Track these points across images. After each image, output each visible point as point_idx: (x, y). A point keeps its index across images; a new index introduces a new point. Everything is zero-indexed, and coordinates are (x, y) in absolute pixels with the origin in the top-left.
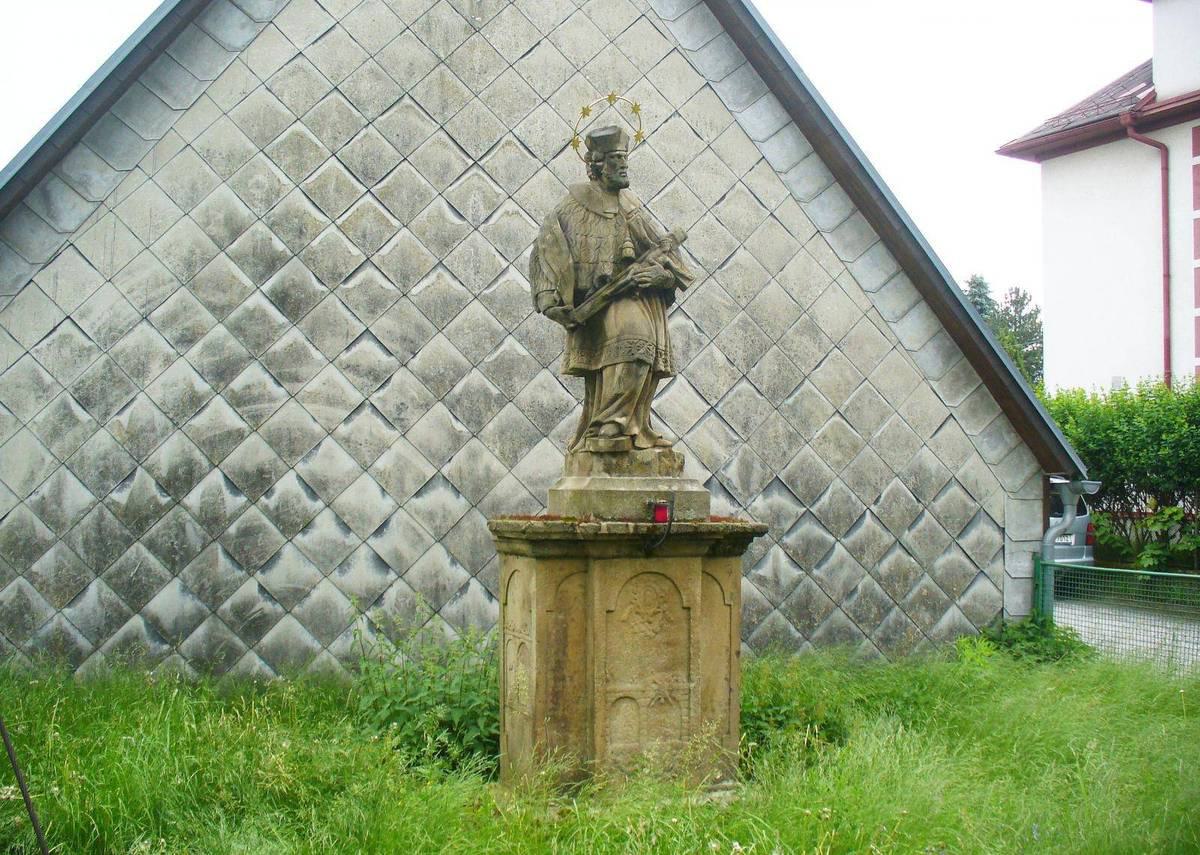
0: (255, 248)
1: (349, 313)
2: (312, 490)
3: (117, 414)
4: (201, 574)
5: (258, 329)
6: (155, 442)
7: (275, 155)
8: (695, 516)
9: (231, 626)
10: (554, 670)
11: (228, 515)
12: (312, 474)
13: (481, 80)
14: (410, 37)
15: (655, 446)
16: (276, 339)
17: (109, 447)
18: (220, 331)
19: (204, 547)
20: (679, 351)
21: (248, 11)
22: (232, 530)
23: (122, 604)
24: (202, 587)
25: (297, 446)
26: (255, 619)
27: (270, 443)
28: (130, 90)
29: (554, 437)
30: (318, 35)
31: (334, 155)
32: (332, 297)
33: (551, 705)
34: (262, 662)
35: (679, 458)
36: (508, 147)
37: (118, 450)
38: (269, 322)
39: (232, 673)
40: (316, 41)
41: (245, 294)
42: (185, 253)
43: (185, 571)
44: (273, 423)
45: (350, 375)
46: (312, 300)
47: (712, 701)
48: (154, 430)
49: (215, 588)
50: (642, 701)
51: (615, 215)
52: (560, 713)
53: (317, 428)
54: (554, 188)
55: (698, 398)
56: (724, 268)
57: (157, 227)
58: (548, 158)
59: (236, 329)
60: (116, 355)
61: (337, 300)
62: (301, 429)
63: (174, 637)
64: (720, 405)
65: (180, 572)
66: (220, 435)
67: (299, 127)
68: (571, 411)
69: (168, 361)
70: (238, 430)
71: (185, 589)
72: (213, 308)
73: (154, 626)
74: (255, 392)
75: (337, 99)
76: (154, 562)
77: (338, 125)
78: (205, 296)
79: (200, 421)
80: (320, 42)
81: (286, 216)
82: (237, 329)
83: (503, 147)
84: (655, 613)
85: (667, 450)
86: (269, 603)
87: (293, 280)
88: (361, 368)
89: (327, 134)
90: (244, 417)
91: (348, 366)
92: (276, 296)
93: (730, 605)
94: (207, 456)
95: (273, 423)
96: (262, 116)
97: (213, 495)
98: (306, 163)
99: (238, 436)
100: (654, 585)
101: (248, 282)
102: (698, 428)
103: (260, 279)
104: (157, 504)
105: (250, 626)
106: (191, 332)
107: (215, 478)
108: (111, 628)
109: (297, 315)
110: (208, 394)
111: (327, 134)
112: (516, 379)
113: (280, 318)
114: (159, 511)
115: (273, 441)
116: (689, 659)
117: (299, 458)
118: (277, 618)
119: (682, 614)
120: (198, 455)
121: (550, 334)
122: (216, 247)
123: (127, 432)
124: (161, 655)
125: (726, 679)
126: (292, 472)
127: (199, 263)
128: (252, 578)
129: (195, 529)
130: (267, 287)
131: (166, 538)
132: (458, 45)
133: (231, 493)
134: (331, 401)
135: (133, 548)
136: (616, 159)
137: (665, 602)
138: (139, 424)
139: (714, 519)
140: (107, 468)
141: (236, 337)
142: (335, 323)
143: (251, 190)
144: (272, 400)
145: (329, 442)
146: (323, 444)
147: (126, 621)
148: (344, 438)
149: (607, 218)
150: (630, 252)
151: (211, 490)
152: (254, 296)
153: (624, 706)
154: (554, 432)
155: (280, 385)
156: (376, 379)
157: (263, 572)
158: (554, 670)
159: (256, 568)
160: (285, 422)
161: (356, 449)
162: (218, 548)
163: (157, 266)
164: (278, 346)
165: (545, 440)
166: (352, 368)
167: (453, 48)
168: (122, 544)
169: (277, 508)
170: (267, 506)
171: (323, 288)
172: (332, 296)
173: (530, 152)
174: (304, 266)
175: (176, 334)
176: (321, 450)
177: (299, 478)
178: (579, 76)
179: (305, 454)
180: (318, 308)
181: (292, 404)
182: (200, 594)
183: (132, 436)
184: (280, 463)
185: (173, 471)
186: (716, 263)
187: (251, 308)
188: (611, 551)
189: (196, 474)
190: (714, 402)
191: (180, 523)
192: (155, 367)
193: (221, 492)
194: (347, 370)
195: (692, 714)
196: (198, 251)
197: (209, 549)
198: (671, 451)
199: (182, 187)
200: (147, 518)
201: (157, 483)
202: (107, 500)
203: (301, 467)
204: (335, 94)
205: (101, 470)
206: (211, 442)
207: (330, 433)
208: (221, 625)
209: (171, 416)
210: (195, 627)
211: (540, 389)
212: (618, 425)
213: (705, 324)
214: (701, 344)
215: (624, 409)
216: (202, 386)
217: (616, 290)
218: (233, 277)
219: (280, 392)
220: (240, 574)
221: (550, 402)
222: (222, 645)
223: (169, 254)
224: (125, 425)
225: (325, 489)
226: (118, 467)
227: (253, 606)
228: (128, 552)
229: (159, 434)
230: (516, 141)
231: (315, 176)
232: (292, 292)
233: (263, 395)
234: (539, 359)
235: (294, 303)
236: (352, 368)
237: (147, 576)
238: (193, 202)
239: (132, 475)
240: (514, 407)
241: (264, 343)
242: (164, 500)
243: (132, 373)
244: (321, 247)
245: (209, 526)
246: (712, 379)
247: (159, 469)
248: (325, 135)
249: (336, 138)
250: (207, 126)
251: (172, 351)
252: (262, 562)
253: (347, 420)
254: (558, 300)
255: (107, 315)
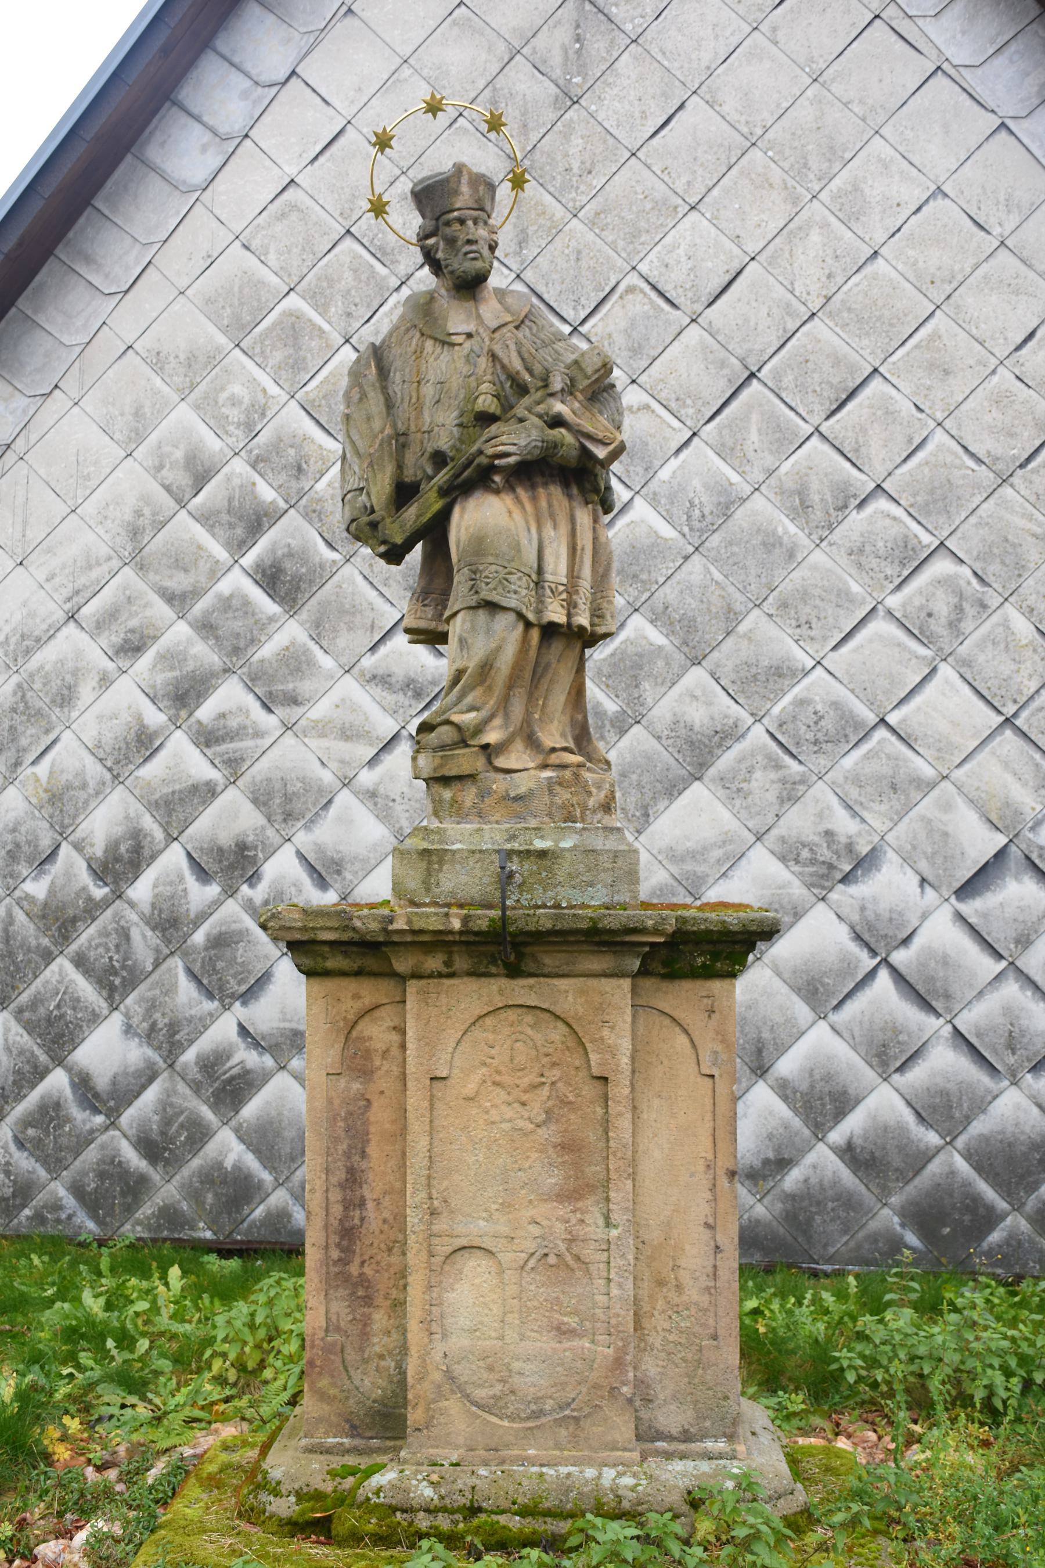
0: (230, 500)
1: (375, 593)
2: (320, 875)
3: (33, 763)
4: (152, 1006)
5: (237, 625)
6: (86, 802)
7: (257, 350)
8: (606, 900)
9: (196, 1088)
10: (342, 1186)
11: (192, 916)
12: (320, 849)
13: (582, 188)
14: (466, 130)
15: (545, 766)
16: (263, 639)
17: (22, 814)
18: (181, 631)
19: (157, 965)
20: (943, 621)
21: (211, 123)
22: (199, 937)
23: (38, 1052)
24: (153, 1027)
25: (297, 806)
26: (232, 1078)
27: (255, 801)
28: (44, 270)
29: (713, 780)
30: (318, 148)
31: (347, 341)
32: (348, 567)
33: (335, 1254)
34: (243, 1147)
35: (599, 788)
36: (630, 297)
37: (34, 818)
38: (253, 614)
39: (196, 1163)
40: (316, 158)
41: (216, 573)
42: (128, 517)
43: (129, 1001)
44: (260, 770)
45: (378, 691)
46: (319, 576)
47: (676, 1267)
48: (84, 786)
49: (173, 1028)
50: (506, 1257)
51: (469, 336)
52: (354, 1269)
53: (327, 777)
54: (711, 357)
55: (981, 705)
56: (1030, 467)
57: (87, 478)
58: (699, 307)
59: (204, 626)
60: (31, 676)
61: (356, 572)
62: (303, 780)
63: (112, 1103)
64: (1025, 714)
65: (122, 1001)
66: (180, 791)
67: (294, 301)
68: (743, 736)
69: (105, 681)
70: (208, 783)
71: (128, 1030)
72: (170, 598)
73: (83, 1083)
74: (233, 723)
75: (351, 251)
76: (85, 989)
77: (353, 292)
78: (158, 578)
79: (152, 771)
80: (322, 159)
81: (277, 446)
82: (206, 628)
83: (621, 297)
84: (535, 1087)
85: (568, 774)
86: (254, 1053)
87: (289, 545)
88: (393, 680)
89: (335, 310)
90: (216, 762)
91: (374, 677)
92: (264, 571)
93: (712, 1076)
94: (161, 824)
95: (260, 770)
96: (236, 289)
97: (171, 883)
98: (304, 359)
99: (208, 792)
100: (529, 1031)
101: (221, 553)
102: (980, 757)
103: (239, 547)
104: (90, 899)
105: (224, 1089)
106: (137, 636)
107: (174, 858)
108: (22, 1087)
109: (294, 600)
110: (163, 728)
111: (335, 310)
112: (646, 685)
113: (268, 606)
114: (92, 909)
115: (260, 799)
116: (608, 1180)
117: (299, 824)
118: (266, 1077)
119: (590, 1090)
120: (149, 823)
121: (705, 606)
122: (172, 503)
123: (46, 791)
124: (92, 1131)
125: (707, 1225)
126: (288, 845)
127: (149, 528)
128: (227, 1013)
129: (144, 936)
130: (249, 559)
131: (101, 950)
132: (543, 130)
133: (197, 880)
134: (347, 734)
135: (54, 966)
136: (457, 226)
137: (554, 1064)
138: (64, 777)
139: (646, 905)
140: (18, 845)
141: (205, 639)
142: (354, 611)
143: (223, 410)
144: (258, 734)
145: (345, 797)
146: (337, 800)
147: (42, 1078)
148: (368, 791)
149: (453, 345)
150: (486, 402)
151: (168, 875)
152: (230, 576)
153: (474, 1267)
154: (712, 772)
155: (270, 710)
156: (418, 695)
157: (244, 1004)
158: (342, 1186)
159: (234, 997)
160: (277, 767)
161: (387, 808)
162: (177, 964)
163: (91, 536)
164: (268, 650)
165: (697, 784)
166: (380, 680)
167: (534, 137)
168: (39, 959)
169: (266, 903)
170: (250, 900)
171: (335, 556)
172: (348, 566)
173: (668, 301)
174: (306, 525)
175: (117, 639)
176: (333, 810)
177: (301, 856)
178: (756, 154)
179: (308, 816)
180: (328, 586)
181: (289, 739)
182: (150, 1036)
183: (54, 796)
184: (270, 832)
185: (112, 848)
186: (1014, 458)
187: (227, 593)
188: (434, 963)
189: (146, 852)
190: (1010, 710)
191: (123, 927)
192: (86, 692)
193: (181, 879)
194: (372, 684)
195: (615, 1291)
196: (147, 511)
197: (164, 967)
198: (576, 776)
199: (122, 414)
200: (74, 920)
201: (90, 866)
202: (17, 893)
203: (302, 839)
204: (348, 243)
205: (8, 848)
206: (167, 803)
207: (347, 783)
208: (182, 1087)
209: (109, 764)
210: (144, 1087)
211: (688, 699)
212: (458, 727)
213: (993, 570)
214: (984, 606)
215: (469, 699)
216: (155, 717)
217: (457, 476)
218: (200, 547)
219: (269, 721)
220: (213, 1005)
221: (705, 721)
222: (181, 1119)
223: (106, 517)
224: (44, 780)
225: (339, 872)
226: (34, 843)
227: (228, 1058)
228: (47, 973)
229: (91, 791)
230: (647, 288)
231: (319, 377)
232: (288, 565)
233: (245, 728)
234: (685, 649)
235: (290, 582)
236: (380, 680)
237: (74, 1009)
238: (138, 436)
239: (51, 856)
240: (645, 732)
241: (247, 646)
242: (99, 892)
243: (53, 701)
244: (331, 491)
245: (164, 930)
246: (1007, 668)
247: (92, 845)
248: (333, 310)
249: (349, 315)
250: (155, 315)
251: (110, 666)
252: (243, 988)
253: (373, 762)
254: (368, 505)
255: (17, 617)
